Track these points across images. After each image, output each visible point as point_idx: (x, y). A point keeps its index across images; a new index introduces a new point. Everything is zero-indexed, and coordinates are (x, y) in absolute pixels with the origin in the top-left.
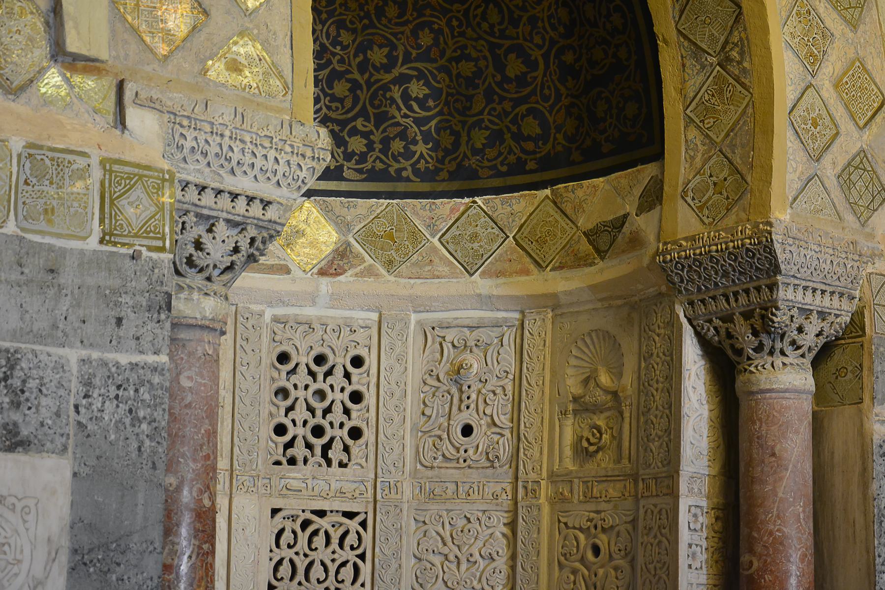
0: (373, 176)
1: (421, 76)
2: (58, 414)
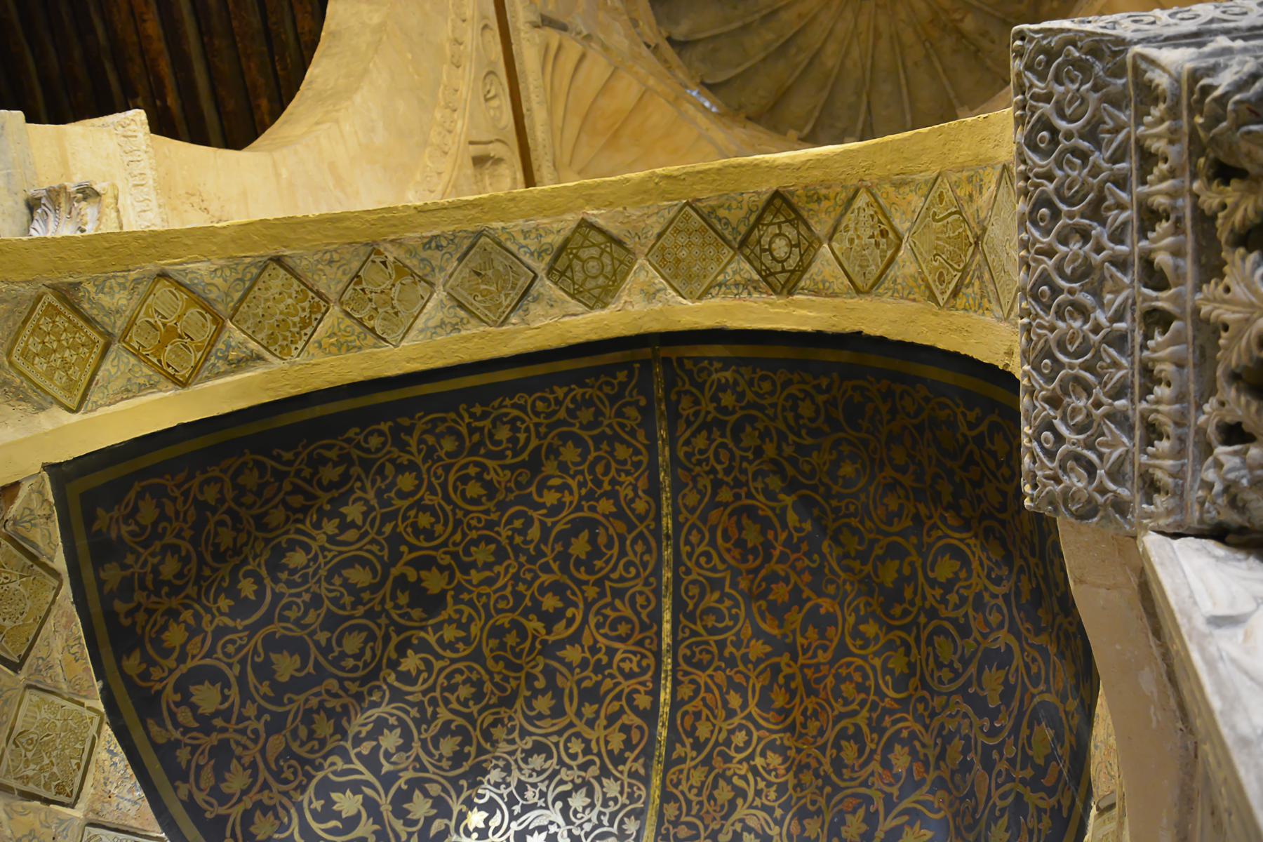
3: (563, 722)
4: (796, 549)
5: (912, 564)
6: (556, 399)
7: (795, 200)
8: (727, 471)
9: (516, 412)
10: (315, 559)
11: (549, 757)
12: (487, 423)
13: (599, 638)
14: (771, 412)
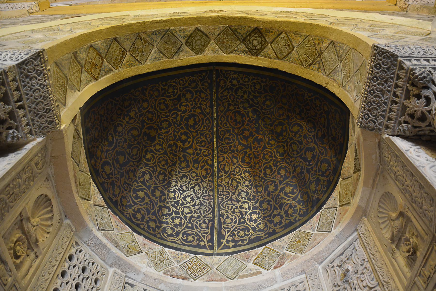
0: (286, 226)
1: (287, 184)
3: (189, 169)
4: (251, 122)
5: (286, 127)
6: (185, 80)
7: (262, 31)
8: (232, 102)
9: (174, 84)
10: (124, 128)
11: (187, 178)
12: (166, 87)
13: (197, 146)
14: (247, 86)
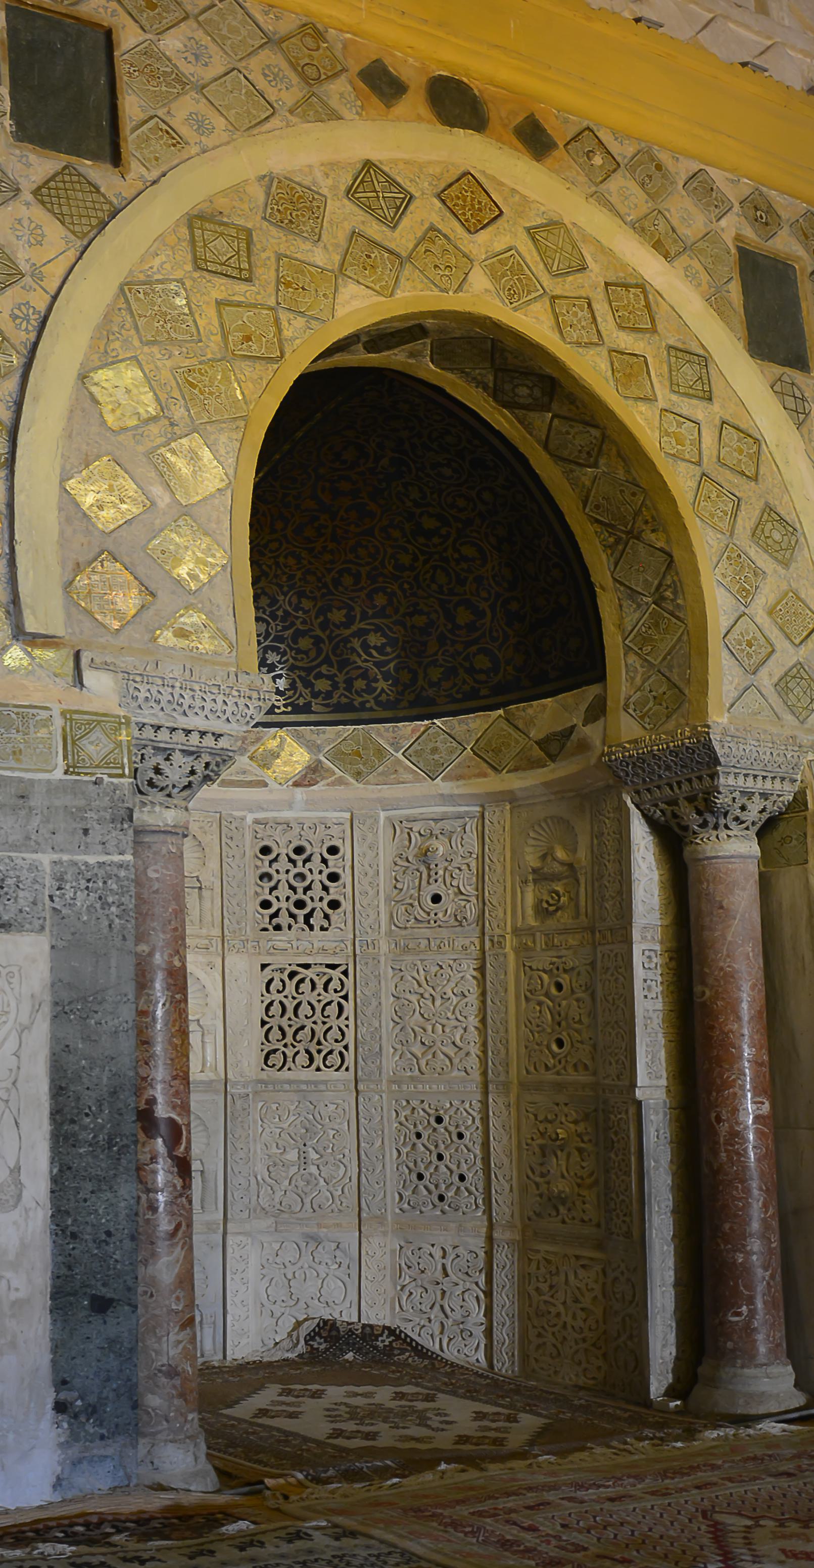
2: (34, 903)
